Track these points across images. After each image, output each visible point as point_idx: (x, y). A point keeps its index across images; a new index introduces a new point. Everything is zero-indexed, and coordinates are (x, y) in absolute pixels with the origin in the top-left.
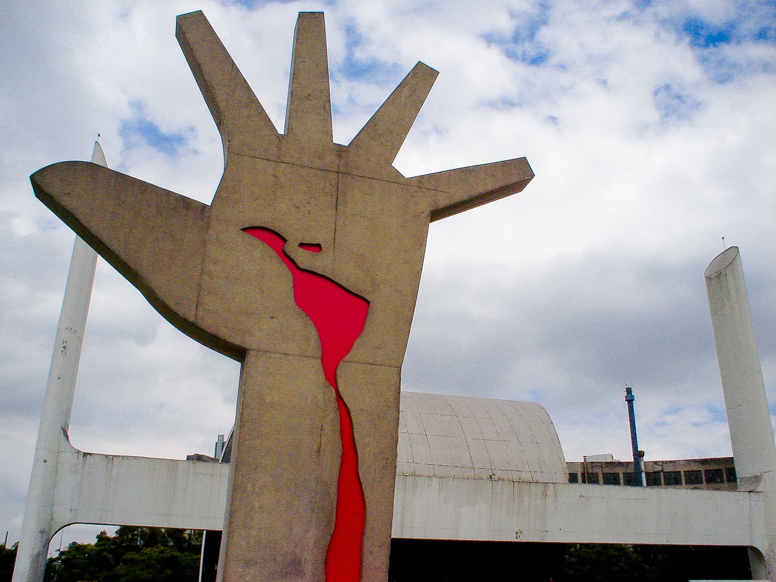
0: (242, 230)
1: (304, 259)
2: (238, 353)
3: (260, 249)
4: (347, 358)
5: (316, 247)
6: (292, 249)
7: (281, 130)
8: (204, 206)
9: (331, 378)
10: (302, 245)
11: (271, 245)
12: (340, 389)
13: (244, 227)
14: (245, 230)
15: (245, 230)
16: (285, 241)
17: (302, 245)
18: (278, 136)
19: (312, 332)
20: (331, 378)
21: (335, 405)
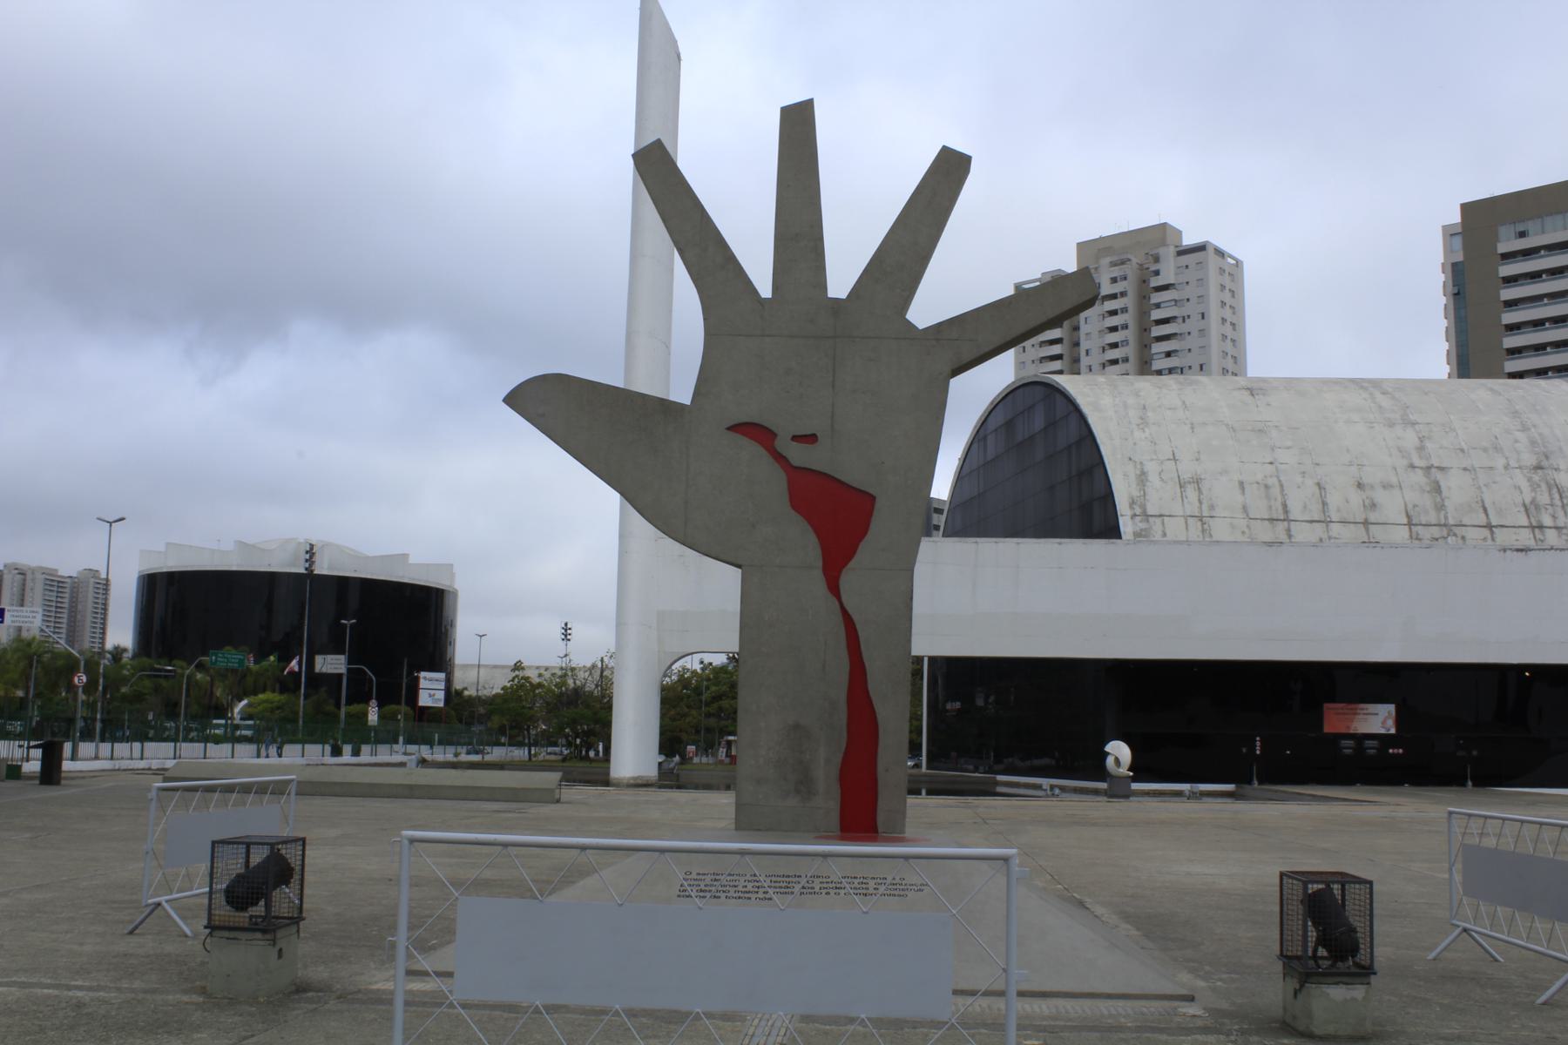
1: (799, 455)
2: (739, 566)
3: (750, 450)
4: (852, 564)
5: (810, 439)
9: (834, 588)
10: (795, 438)
11: (761, 443)
13: (728, 426)
14: (729, 429)
16: (774, 435)
17: (795, 438)
20: (834, 588)
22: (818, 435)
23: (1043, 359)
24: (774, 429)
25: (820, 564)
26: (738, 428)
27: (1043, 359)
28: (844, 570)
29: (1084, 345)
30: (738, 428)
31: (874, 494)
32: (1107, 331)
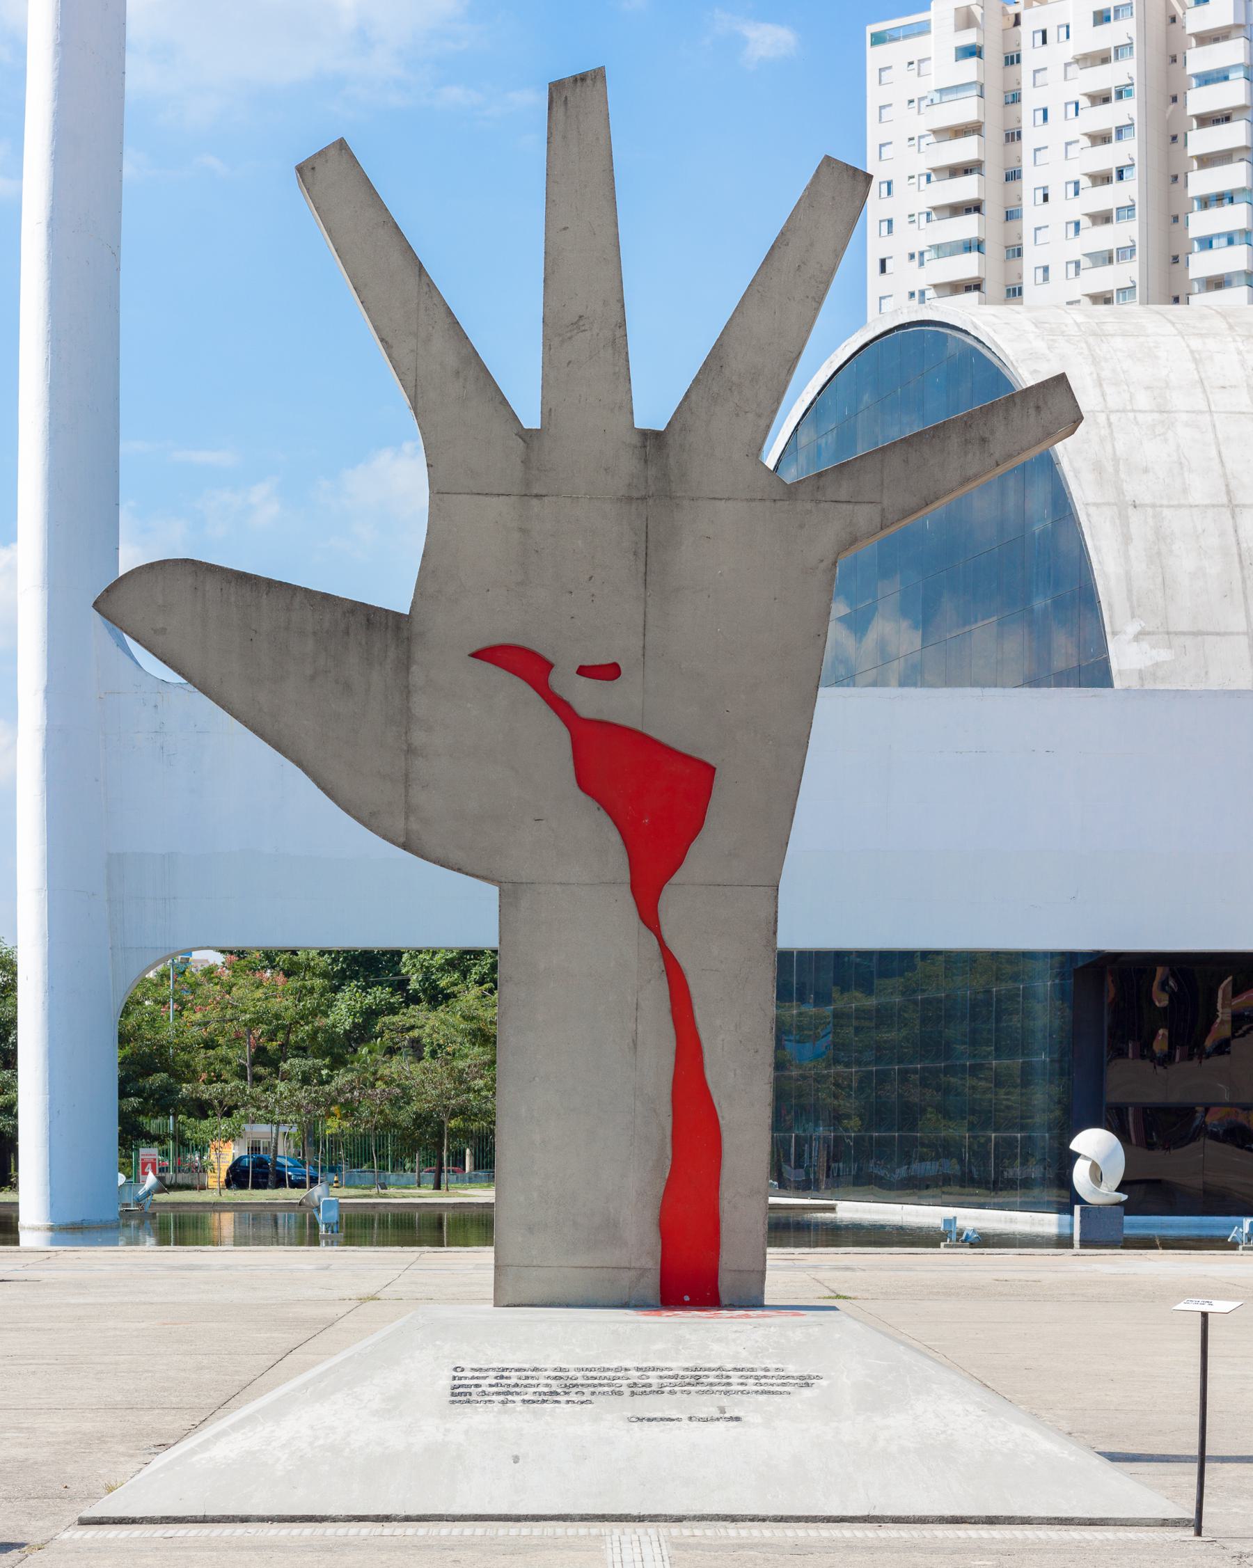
0: (469, 655)
4: (676, 878)
5: (609, 672)
6: (566, 683)
7: (531, 418)
8: (398, 616)
10: (583, 671)
12: (666, 935)
13: (474, 650)
14: (476, 655)
15: (476, 655)
16: (549, 666)
17: (583, 671)
18: (527, 436)
19: (614, 837)
20: (649, 916)
21: (659, 965)
22: (622, 667)
23: (942, 250)
24: (549, 656)
25: (627, 877)
26: (488, 655)
27: (942, 250)
28: (666, 887)
29: (1031, 99)
30: (488, 655)
31: (712, 762)
32: (1086, 142)
